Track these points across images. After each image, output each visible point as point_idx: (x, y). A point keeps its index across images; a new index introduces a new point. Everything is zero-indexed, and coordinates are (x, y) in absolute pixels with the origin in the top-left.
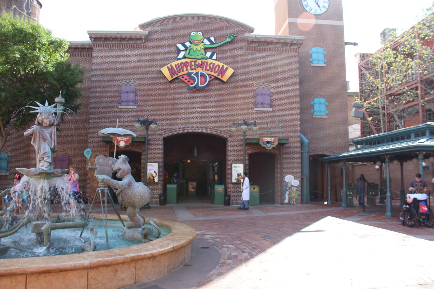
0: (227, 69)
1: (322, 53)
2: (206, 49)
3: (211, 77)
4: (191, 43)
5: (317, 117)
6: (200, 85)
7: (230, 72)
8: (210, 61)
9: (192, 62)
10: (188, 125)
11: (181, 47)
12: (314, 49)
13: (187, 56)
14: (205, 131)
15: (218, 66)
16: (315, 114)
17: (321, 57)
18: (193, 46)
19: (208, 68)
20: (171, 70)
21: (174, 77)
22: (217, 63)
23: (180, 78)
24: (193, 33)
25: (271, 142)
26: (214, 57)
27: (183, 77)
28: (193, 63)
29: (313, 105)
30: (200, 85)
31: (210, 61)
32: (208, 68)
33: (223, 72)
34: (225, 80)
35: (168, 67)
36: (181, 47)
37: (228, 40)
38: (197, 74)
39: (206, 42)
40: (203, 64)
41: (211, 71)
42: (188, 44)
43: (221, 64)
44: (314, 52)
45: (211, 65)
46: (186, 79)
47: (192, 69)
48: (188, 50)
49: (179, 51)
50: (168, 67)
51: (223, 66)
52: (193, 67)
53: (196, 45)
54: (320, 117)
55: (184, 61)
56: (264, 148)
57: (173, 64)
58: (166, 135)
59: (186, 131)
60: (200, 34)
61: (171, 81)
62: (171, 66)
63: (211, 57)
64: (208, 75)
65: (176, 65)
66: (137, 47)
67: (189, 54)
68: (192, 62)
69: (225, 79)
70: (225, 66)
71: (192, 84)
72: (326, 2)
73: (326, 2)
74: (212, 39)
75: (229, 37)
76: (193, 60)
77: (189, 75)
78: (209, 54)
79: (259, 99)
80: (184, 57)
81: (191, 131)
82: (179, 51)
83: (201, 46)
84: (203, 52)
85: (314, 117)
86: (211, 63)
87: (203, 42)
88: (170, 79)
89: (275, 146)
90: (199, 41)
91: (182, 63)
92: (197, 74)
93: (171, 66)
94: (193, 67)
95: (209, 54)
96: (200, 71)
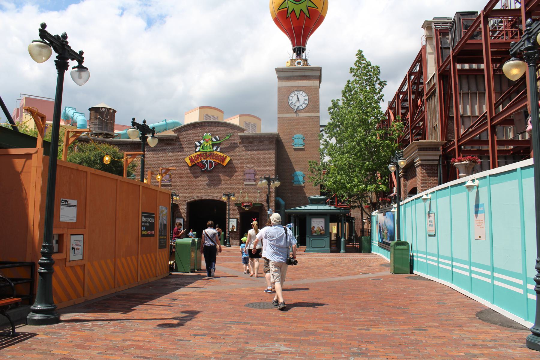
0: (226, 157)
1: (302, 139)
2: (213, 145)
3: (216, 163)
4: (204, 141)
5: (296, 185)
6: (208, 169)
7: (228, 159)
8: (216, 152)
9: (204, 153)
10: (202, 194)
11: (198, 144)
12: (296, 136)
13: (201, 150)
14: (212, 198)
15: (220, 155)
16: (295, 183)
17: (301, 141)
18: (205, 143)
19: (214, 157)
20: (191, 159)
21: (193, 164)
22: (220, 154)
23: (197, 164)
24: (205, 134)
25: (248, 205)
26: (219, 150)
27: (198, 164)
28: (205, 155)
29: (293, 177)
30: (208, 169)
31: (216, 152)
32: (214, 157)
33: (224, 159)
34: (225, 165)
35: (189, 158)
36: (198, 144)
37: (227, 138)
38: (207, 162)
39: (214, 140)
40: (211, 154)
41: (216, 159)
42: (202, 141)
43: (222, 154)
44: (295, 139)
45: (216, 155)
46: (200, 165)
47: (204, 159)
48: (202, 146)
49: (197, 146)
50: (189, 158)
51: (223, 155)
52: (205, 157)
53: (207, 142)
54: (298, 185)
55: (199, 153)
56: (244, 209)
57: (192, 156)
58: (189, 201)
59: (201, 198)
60: (209, 134)
61: (192, 166)
62: (191, 156)
63: (216, 150)
64: (214, 162)
65: (194, 156)
66: (171, 144)
67: (202, 149)
68: (204, 153)
69: (225, 164)
70: (225, 156)
71: (204, 168)
72: (307, 100)
73: (307, 100)
74: (217, 137)
75: (228, 136)
76: (205, 152)
77: (202, 162)
78: (215, 148)
79: (248, 177)
80: (199, 151)
81: (204, 198)
82: (197, 146)
83: (210, 143)
84: (211, 147)
85: (294, 185)
86: (216, 154)
87: (211, 140)
88: (190, 165)
89: (250, 208)
90: (209, 139)
91: (198, 155)
92: (207, 162)
93: (191, 156)
94: (205, 157)
95: (215, 148)
96: (209, 160)
